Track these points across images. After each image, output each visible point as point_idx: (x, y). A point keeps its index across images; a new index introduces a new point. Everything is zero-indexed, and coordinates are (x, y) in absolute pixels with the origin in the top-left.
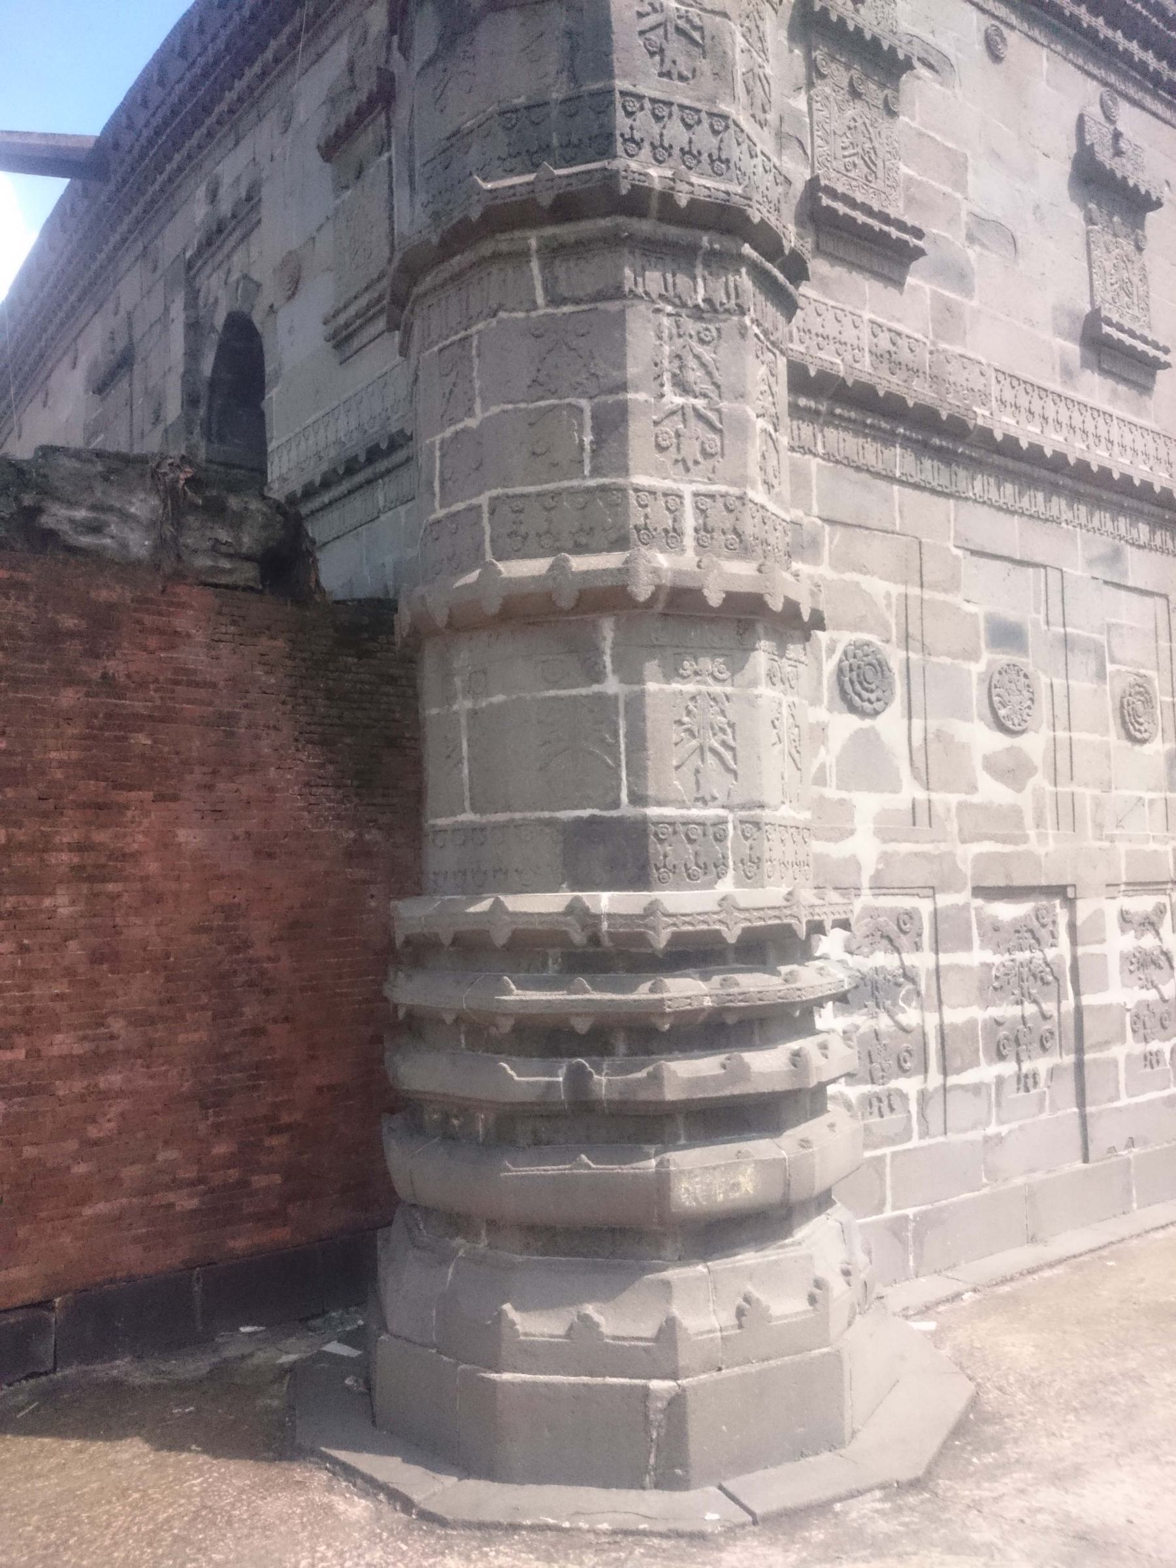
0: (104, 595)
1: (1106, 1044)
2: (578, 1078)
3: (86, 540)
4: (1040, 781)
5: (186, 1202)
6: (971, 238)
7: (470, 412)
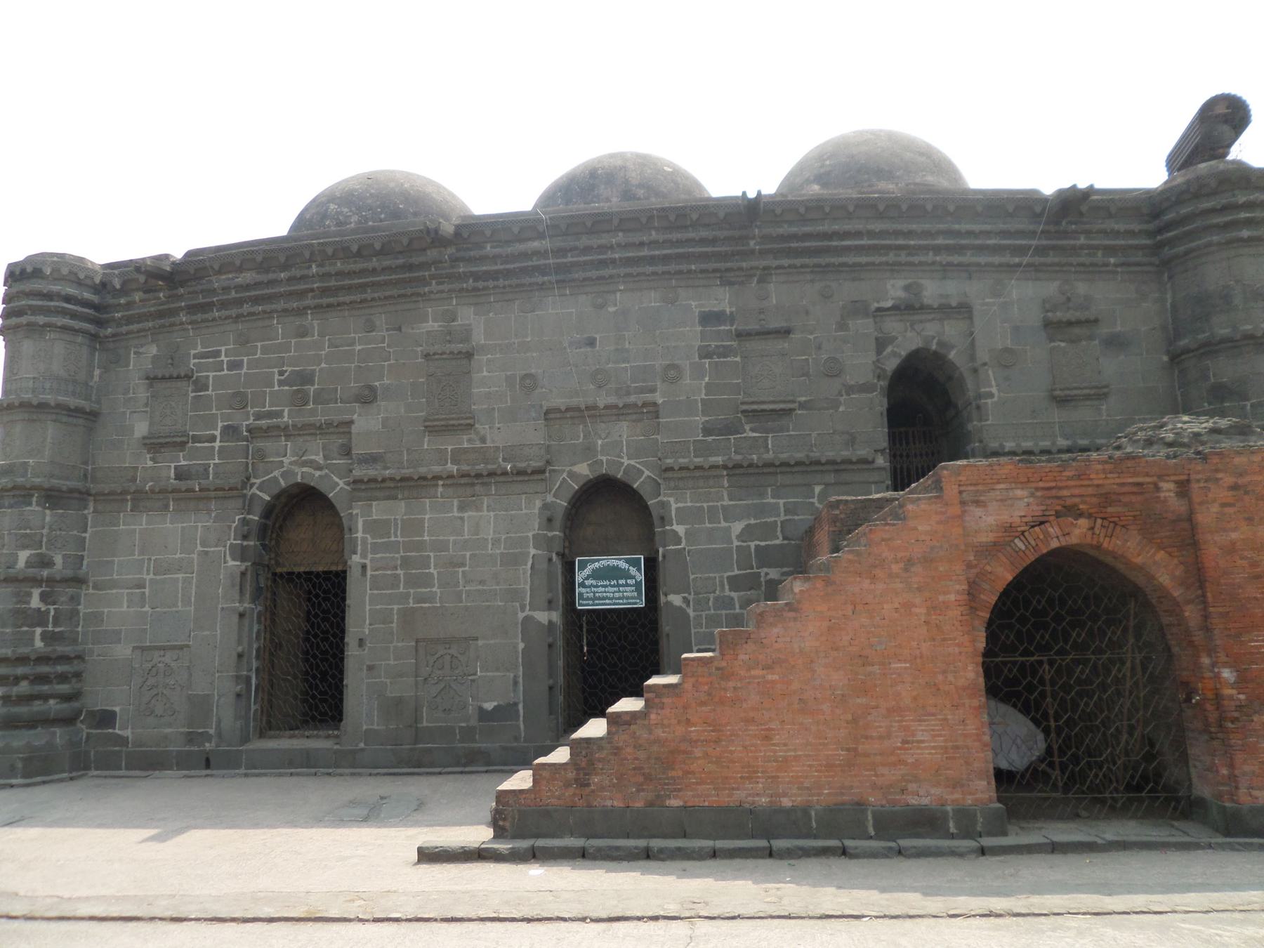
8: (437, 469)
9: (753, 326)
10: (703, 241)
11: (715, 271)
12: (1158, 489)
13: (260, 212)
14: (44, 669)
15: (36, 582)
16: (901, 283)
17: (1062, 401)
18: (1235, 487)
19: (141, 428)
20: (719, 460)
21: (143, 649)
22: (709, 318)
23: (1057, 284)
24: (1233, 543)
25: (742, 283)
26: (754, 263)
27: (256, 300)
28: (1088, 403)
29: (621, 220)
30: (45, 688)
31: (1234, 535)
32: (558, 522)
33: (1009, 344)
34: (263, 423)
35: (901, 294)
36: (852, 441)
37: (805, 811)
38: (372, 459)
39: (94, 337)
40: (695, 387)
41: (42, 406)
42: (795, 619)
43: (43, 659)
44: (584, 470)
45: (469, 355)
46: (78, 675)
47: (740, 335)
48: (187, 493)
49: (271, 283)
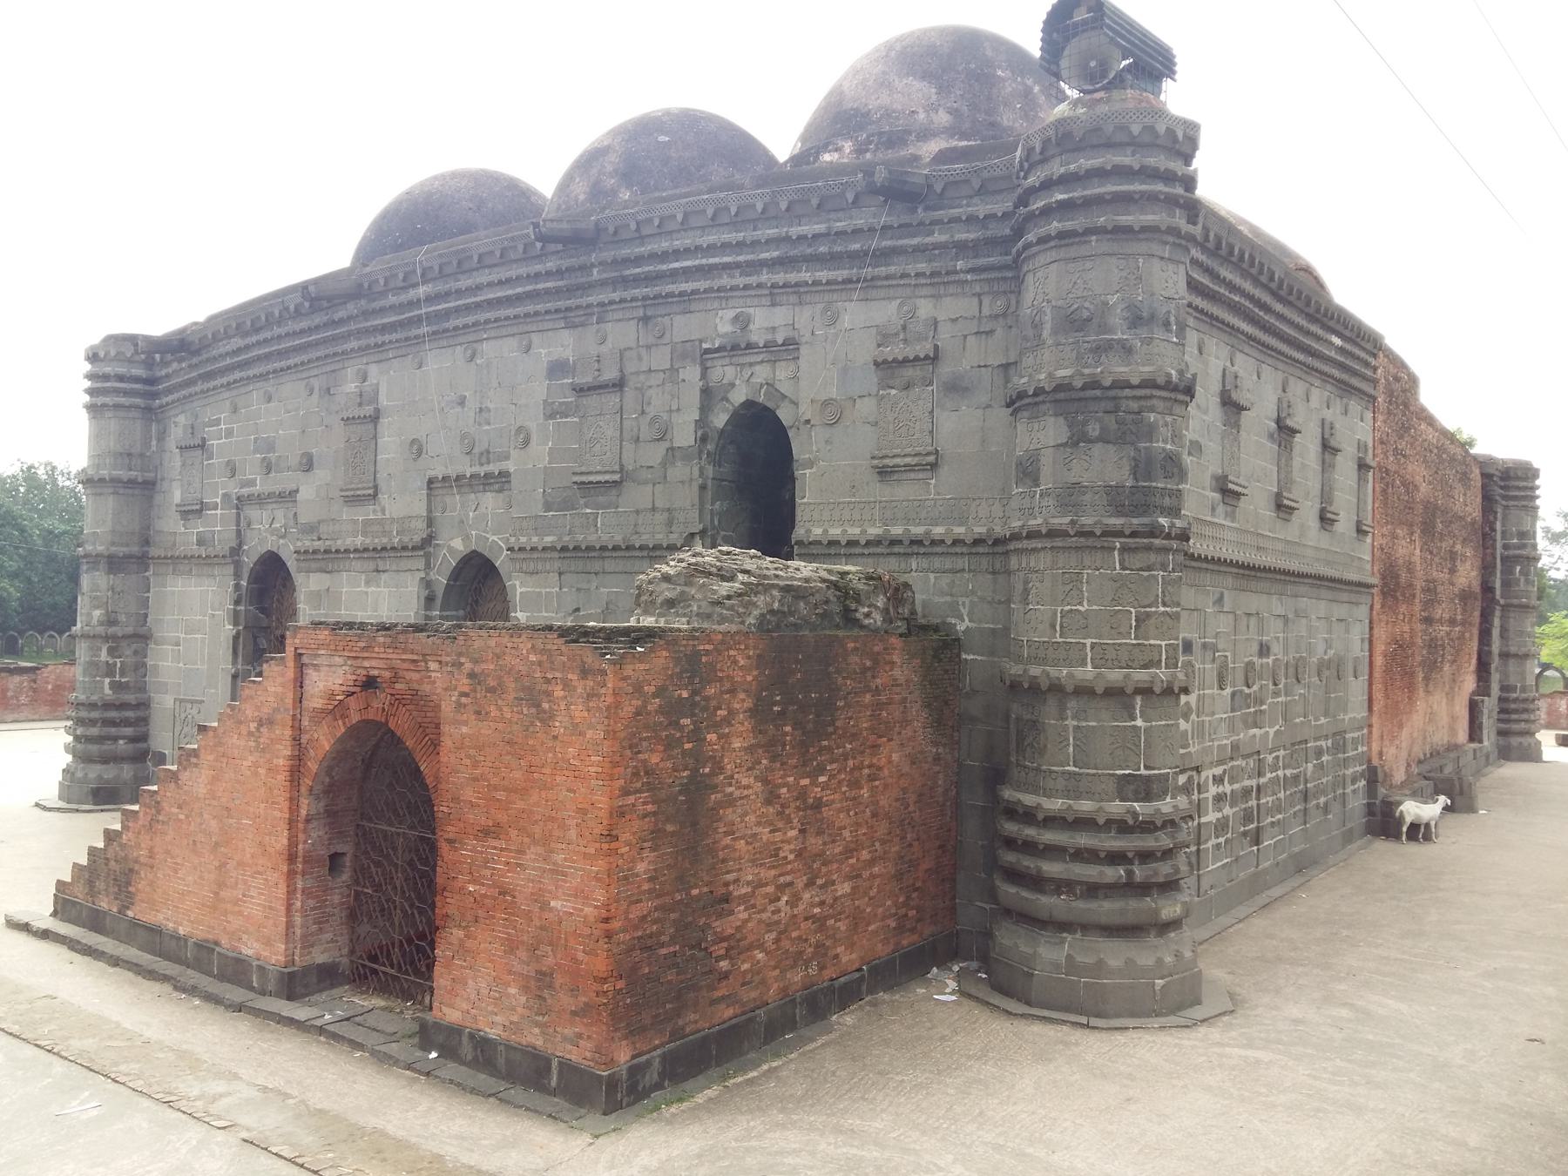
0: (876, 649)
1: (1206, 841)
2: (1130, 873)
3: (867, 622)
4: (1193, 716)
5: (893, 924)
6: (1190, 454)
7: (1081, 604)
8: (349, 541)
9: (587, 379)
10: (549, 274)
11: (557, 311)
12: (427, 670)
13: (326, 247)
14: (113, 714)
15: (107, 638)
16: (731, 314)
17: (884, 473)
18: (472, 675)
19: (177, 496)
20: (549, 539)
21: (181, 701)
22: (557, 369)
23: (896, 303)
24: (463, 737)
25: (583, 325)
26: (591, 299)
27: (241, 366)
28: (912, 475)
29: (480, 256)
30: (113, 730)
31: (464, 730)
32: (439, 602)
33: (833, 392)
34: (245, 491)
35: (725, 328)
36: (670, 523)
37: (185, 939)
38: (310, 529)
39: (148, 409)
40: (540, 452)
41: (102, 480)
42: (196, 765)
43: (107, 706)
44: (458, 545)
45: (375, 418)
46: (145, 721)
47: (580, 390)
48: (200, 562)
49: (248, 348)
